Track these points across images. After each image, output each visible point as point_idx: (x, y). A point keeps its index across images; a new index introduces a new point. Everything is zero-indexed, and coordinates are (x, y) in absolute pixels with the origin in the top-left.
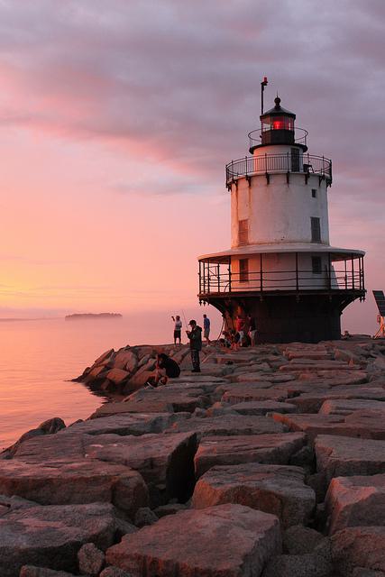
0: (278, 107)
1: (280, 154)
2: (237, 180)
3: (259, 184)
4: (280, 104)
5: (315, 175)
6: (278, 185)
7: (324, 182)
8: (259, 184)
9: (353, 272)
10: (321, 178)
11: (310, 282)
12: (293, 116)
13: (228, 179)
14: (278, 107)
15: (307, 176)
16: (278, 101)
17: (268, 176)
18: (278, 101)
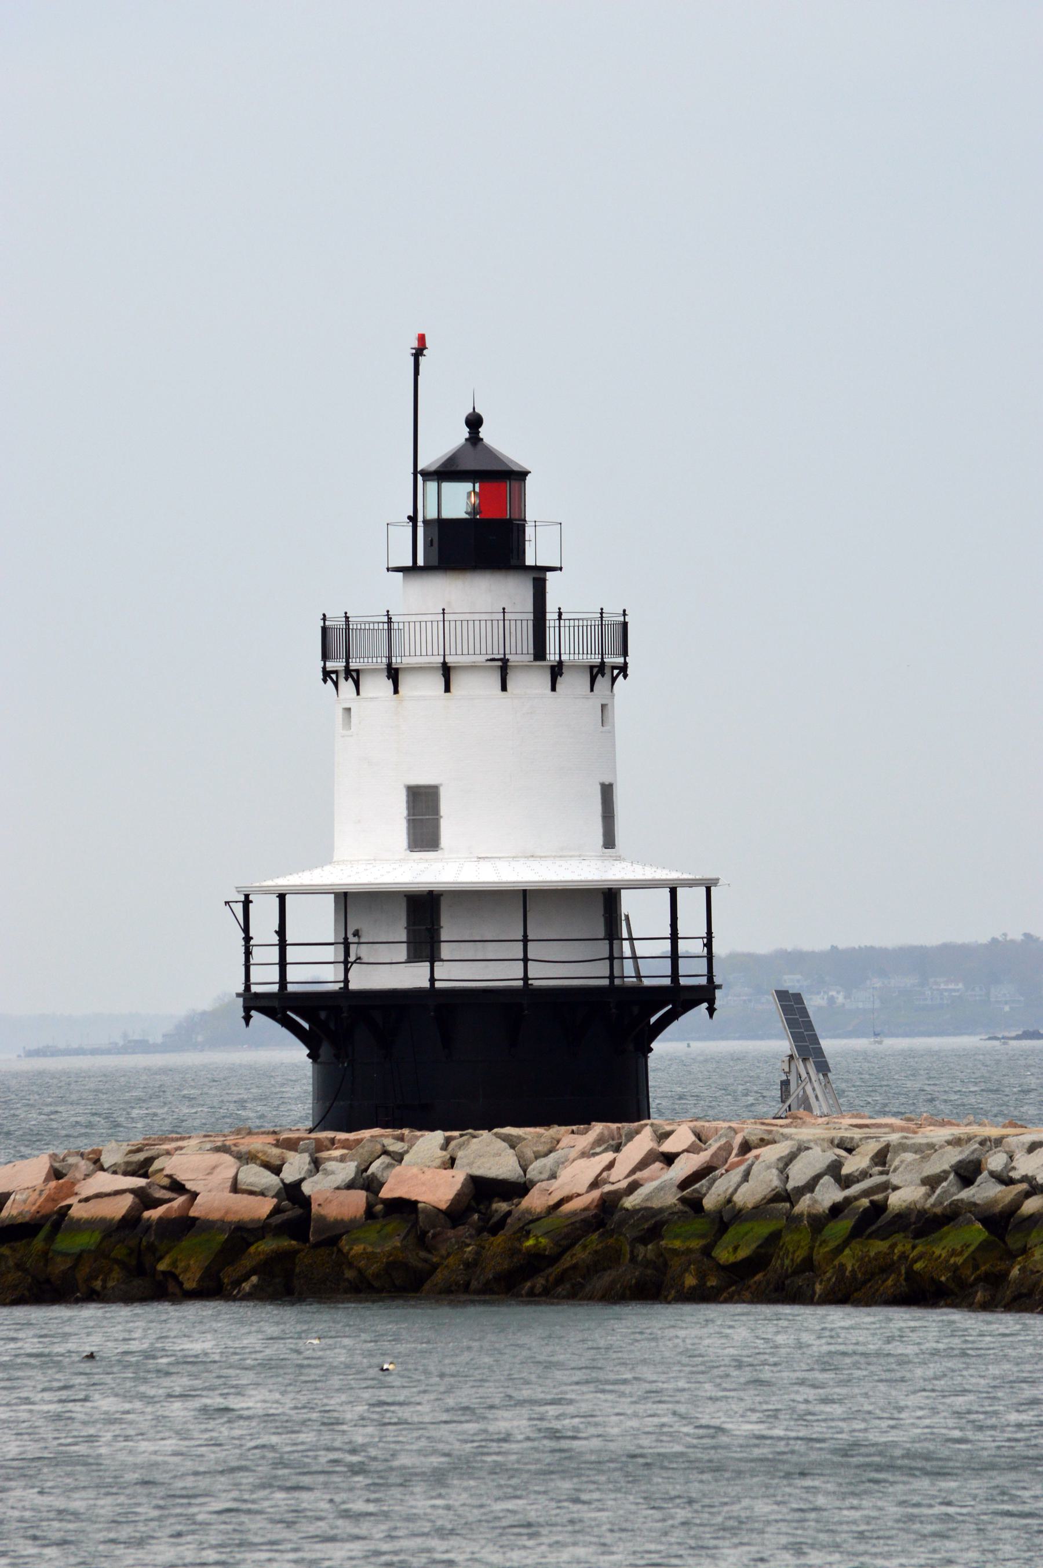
0: (474, 438)
1: (479, 601)
2: (357, 671)
3: (423, 689)
4: (484, 432)
5: (576, 667)
6: (477, 689)
7: (602, 682)
8: (423, 689)
9: (674, 938)
10: (596, 672)
11: (562, 964)
12: (522, 475)
13: (325, 657)
14: (474, 438)
15: (557, 671)
16: (474, 422)
17: (446, 670)
18: (474, 422)
